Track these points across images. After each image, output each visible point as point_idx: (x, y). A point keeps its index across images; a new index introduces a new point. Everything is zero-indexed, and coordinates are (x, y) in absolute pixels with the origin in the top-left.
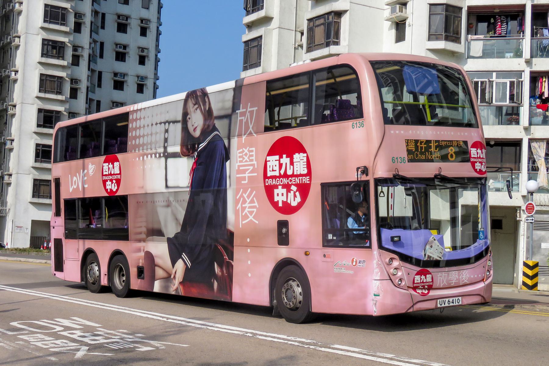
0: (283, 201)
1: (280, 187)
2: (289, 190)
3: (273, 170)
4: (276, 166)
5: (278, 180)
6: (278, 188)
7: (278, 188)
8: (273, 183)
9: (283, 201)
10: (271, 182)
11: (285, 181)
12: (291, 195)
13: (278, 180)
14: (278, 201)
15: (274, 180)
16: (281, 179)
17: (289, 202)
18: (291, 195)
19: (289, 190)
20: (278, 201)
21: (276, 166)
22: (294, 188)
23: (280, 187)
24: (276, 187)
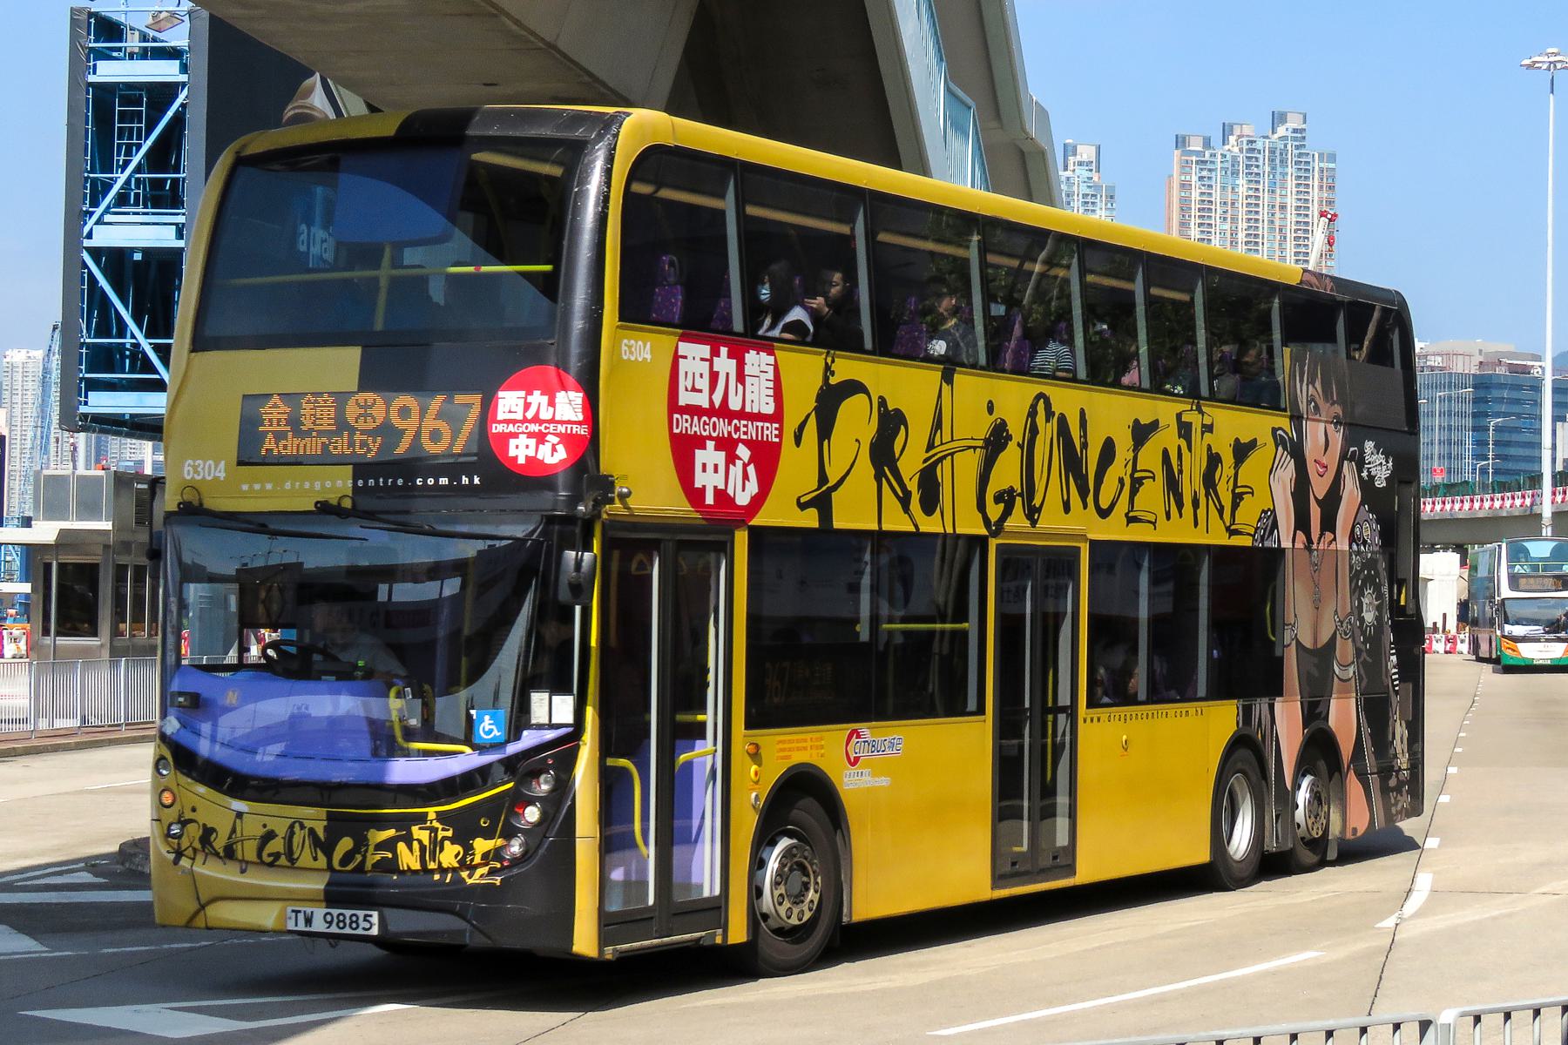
0: (715, 487)
1: (710, 444)
2: (731, 458)
3: (694, 390)
4: (701, 376)
5: (705, 423)
6: (703, 447)
7: (703, 447)
8: (694, 429)
9: (715, 487)
10: (688, 425)
11: (724, 428)
12: (736, 470)
13: (705, 423)
14: (704, 487)
15: (696, 418)
16: (714, 419)
17: (730, 491)
18: (736, 470)
19: (731, 458)
20: (704, 487)
21: (701, 376)
22: (743, 452)
23: (710, 444)
24: (700, 442)
